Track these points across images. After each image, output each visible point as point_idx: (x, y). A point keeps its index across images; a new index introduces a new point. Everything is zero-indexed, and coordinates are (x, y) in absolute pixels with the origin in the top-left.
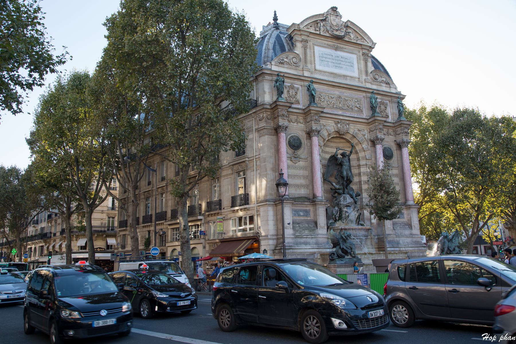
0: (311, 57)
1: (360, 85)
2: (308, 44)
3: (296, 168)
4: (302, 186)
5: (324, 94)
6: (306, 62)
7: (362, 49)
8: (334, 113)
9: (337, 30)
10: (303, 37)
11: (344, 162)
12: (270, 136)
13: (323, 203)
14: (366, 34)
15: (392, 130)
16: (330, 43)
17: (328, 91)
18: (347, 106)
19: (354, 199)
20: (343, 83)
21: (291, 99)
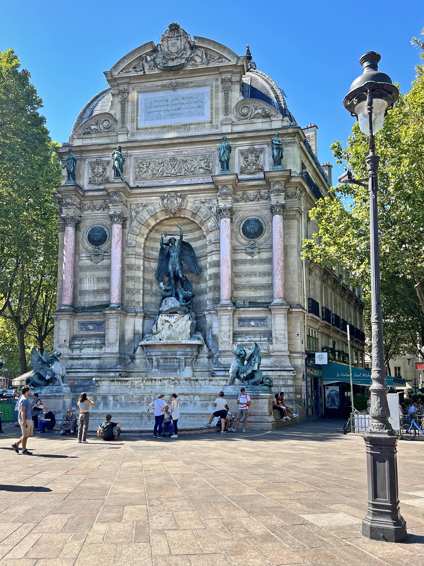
0: (133, 112)
1: (214, 131)
2: (130, 96)
3: (97, 268)
4: (105, 292)
6: (123, 121)
7: (220, 73)
8: (162, 185)
9: (173, 60)
10: (121, 88)
12: (63, 233)
14: (224, 48)
15: (267, 191)
16: (165, 82)
17: (155, 155)
20: (199, 134)
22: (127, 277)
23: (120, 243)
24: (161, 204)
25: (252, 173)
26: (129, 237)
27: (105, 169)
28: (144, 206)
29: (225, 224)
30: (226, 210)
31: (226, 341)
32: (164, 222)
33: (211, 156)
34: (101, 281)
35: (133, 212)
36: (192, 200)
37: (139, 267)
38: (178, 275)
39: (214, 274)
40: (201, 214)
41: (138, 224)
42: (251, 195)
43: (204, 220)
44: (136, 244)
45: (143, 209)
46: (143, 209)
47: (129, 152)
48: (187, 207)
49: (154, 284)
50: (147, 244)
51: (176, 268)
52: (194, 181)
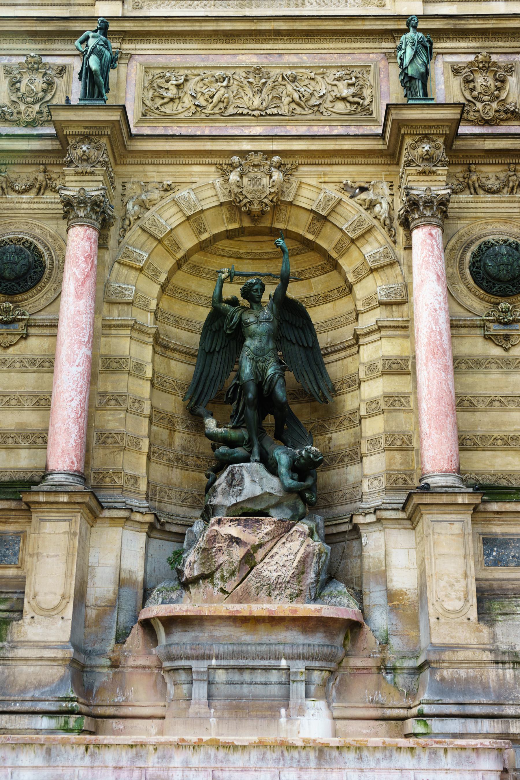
4: (26, 437)
5: (182, 72)
11: (248, 324)
13: (65, 498)
17: (203, 60)
18: (293, 101)
19: (282, 483)
21: (22, 107)
22: (103, 395)
23: (90, 283)
24: (218, 185)
25: (487, 123)
26: (114, 274)
27: (50, 84)
28: (166, 190)
29: (429, 241)
30: (432, 202)
31: (455, 612)
32: (220, 244)
33: (368, 72)
34: (14, 402)
35: (130, 206)
36: (313, 181)
37: (139, 367)
38: (272, 391)
39: (387, 396)
40: (342, 220)
41: (144, 237)
42: (488, 179)
43: (353, 236)
44: (135, 297)
45: (162, 198)
46: (162, 198)
47: (125, 46)
48: (299, 198)
49: (179, 427)
50: (164, 305)
51: (265, 371)
52: (317, 130)
